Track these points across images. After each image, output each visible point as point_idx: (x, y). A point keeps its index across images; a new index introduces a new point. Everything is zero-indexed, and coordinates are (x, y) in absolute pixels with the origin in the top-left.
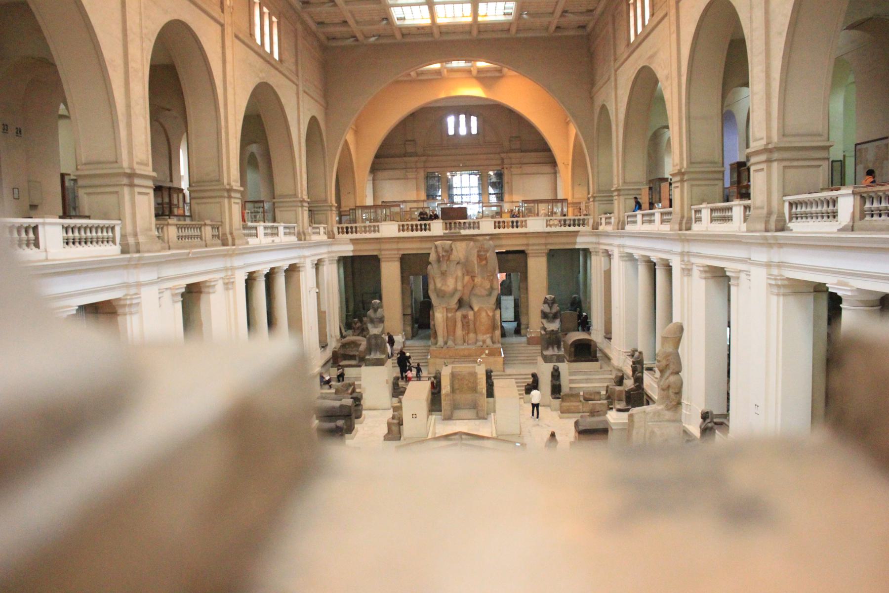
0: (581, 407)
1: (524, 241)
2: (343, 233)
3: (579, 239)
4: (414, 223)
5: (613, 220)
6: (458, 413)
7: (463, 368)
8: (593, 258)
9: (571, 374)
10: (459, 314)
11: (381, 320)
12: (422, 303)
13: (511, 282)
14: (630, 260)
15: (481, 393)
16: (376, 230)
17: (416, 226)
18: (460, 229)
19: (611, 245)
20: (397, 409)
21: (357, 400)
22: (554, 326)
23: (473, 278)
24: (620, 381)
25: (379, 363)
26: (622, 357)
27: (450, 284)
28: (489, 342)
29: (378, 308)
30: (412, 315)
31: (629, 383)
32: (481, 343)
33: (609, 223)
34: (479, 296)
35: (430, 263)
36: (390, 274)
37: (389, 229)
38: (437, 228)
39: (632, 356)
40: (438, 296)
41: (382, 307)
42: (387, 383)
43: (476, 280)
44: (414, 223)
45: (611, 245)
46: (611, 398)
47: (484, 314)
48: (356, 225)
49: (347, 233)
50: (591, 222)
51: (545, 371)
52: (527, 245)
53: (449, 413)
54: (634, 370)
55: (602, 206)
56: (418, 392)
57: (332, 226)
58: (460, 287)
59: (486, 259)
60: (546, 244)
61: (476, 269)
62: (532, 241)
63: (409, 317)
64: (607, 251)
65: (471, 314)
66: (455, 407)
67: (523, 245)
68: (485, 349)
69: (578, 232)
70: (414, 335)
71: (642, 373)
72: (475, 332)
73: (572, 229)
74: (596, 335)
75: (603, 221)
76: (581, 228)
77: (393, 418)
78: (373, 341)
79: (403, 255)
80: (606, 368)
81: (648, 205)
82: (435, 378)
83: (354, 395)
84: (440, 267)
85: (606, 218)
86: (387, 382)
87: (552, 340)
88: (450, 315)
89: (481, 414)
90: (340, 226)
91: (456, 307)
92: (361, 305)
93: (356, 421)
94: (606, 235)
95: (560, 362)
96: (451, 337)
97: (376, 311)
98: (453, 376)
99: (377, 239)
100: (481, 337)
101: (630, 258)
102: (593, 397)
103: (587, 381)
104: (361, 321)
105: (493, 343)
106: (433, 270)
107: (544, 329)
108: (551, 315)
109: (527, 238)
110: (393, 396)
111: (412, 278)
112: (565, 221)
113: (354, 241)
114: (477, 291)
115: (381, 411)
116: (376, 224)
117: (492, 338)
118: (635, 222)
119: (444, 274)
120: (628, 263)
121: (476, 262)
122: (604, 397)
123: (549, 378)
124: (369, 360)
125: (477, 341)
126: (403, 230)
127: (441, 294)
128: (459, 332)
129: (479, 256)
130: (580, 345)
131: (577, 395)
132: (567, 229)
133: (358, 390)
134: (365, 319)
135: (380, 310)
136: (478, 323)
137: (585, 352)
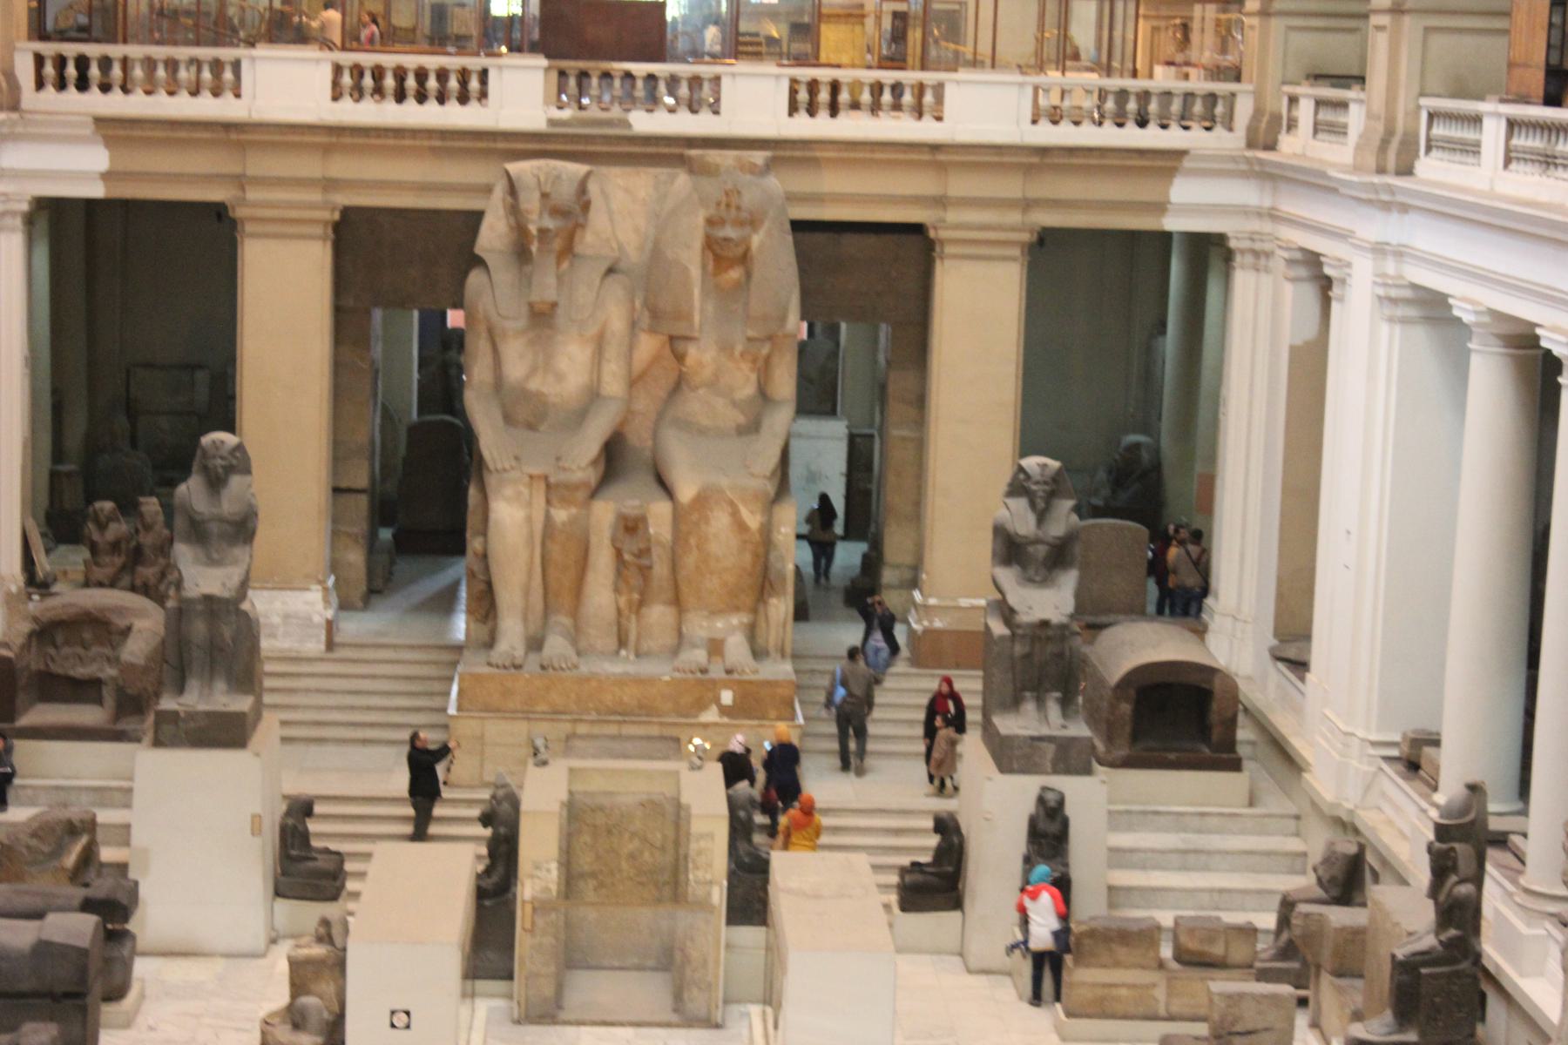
0: (1160, 993)
1: (922, 184)
2: (61, 85)
3: (1182, 191)
4: (411, 61)
5: (1355, 118)
6: (588, 988)
7: (627, 778)
8: (1243, 280)
9: (1117, 820)
10: (604, 513)
11: (243, 529)
12: (413, 430)
13: (834, 354)
14: (1428, 320)
15: (704, 905)
16: (225, 80)
17: (421, 75)
18: (629, 101)
19: (1341, 235)
20: (320, 973)
21: (114, 910)
22: (1050, 602)
23: (676, 344)
24: (1349, 878)
25: (228, 733)
26: (1361, 765)
27: (571, 367)
28: (737, 648)
29: (230, 470)
30: (371, 491)
31: (1405, 914)
32: (700, 656)
33: (1339, 130)
34: (702, 432)
35: (479, 262)
36: (284, 302)
37: (287, 85)
38: (521, 94)
39: (1412, 766)
40: (508, 419)
41: (247, 471)
42: (256, 830)
43: (693, 353)
44: (411, 61)
45: (1341, 235)
46: (1297, 956)
47: (719, 521)
48: (135, 51)
49: (83, 84)
50: (1244, 109)
51: (996, 805)
52: (941, 202)
53: (549, 991)
54: (1442, 866)
55: (1302, 41)
56: (412, 897)
57: (11, 49)
58: (613, 385)
59: (744, 259)
60: (1027, 205)
61: (699, 306)
62: (960, 185)
63: (363, 501)
64: (1313, 260)
65: (659, 514)
66: (573, 957)
67: (917, 200)
68: (715, 686)
69: (1180, 154)
70: (377, 587)
71: (1478, 880)
72: (677, 602)
73: (1151, 137)
74: (1233, 641)
75: (1305, 112)
76: (1194, 138)
77: (295, 1018)
78: (199, 629)
79: (347, 212)
80: (1275, 803)
81: (1536, 80)
82: (486, 819)
83: (101, 888)
84: (525, 281)
85: (1320, 103)
86: (256, 820)
87: (1043, 665)
88: (561, 515)
89: (696, 1001)
90: (49, 49)
91: (592, 476)
92: (121, 422)
93: (108, 1011)
94: (1316, 182)
95: (1069, 771)
96: (566, 621)
97: (216, 483)
98: (576, 814)
99: (228, 126)
100: (700, 626)
101: (1432, 308)
102: (1218, 950)
103: (1187, 858)
104: (128, 507)
105: (758, 653)
106: (494, 294)
107: (1007, 612)
108: (1041, 551)
109: (942, 167)
110: (278, 893)
111: (378, 314)
112: (1122, 95)
113: (111, 130)
114: (695, 405)
115: (219, 965)
116: (226, 53)
117: (751, 632)
118: (1473, 149)
119: (542, 318)
120: (1420, 334)
121: (695, 272)
122: (1264, 945)
123: (1017, 841)
124: (173, 717)
125: (680, 640)
126: (358, 93)
127: (526, 413)
128: (601, 595)
129: (710, 244)
130: (1156, 687)
131: (1147, 936)
132: (1132, 136)
133: (107, 854)
134: (151, 505)
135: (236, 481)
136: (690, 561)
137: (1181, 720)
